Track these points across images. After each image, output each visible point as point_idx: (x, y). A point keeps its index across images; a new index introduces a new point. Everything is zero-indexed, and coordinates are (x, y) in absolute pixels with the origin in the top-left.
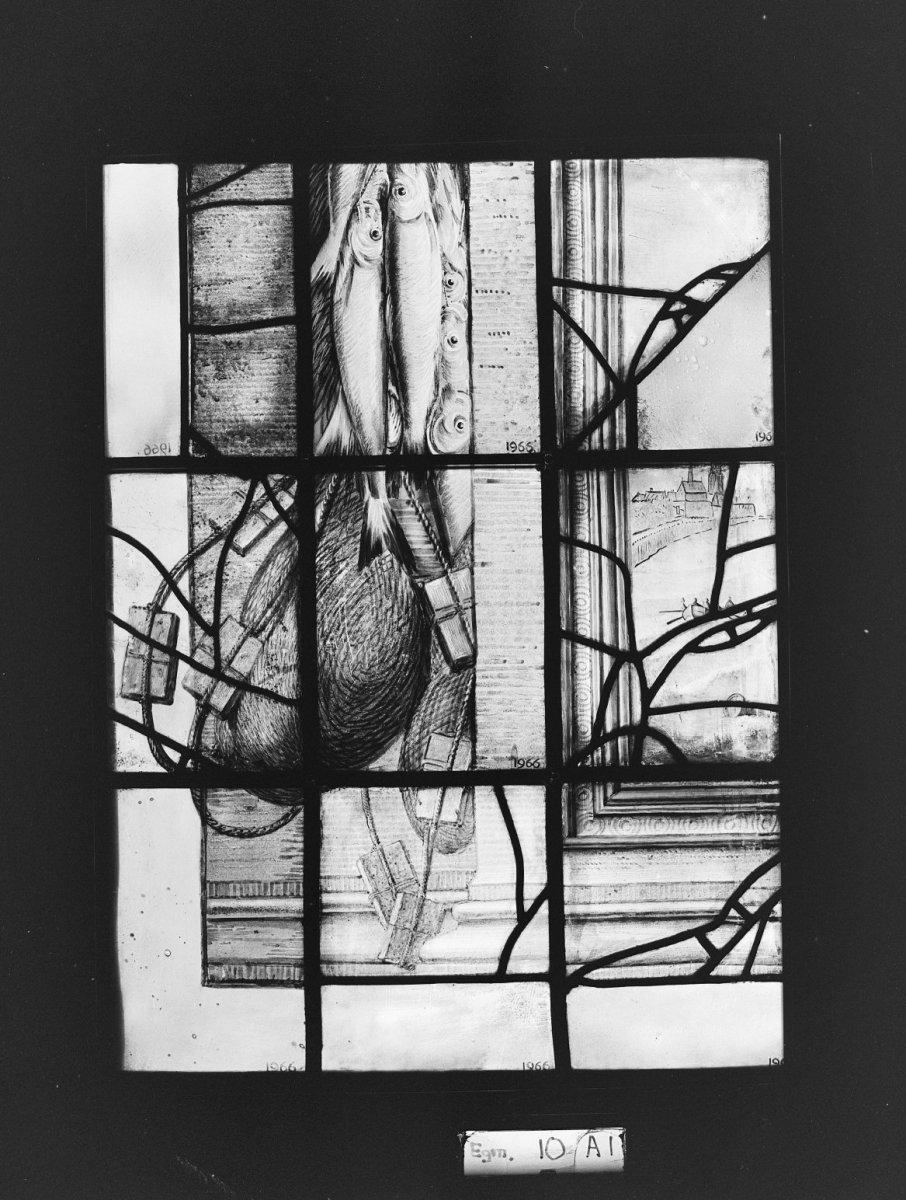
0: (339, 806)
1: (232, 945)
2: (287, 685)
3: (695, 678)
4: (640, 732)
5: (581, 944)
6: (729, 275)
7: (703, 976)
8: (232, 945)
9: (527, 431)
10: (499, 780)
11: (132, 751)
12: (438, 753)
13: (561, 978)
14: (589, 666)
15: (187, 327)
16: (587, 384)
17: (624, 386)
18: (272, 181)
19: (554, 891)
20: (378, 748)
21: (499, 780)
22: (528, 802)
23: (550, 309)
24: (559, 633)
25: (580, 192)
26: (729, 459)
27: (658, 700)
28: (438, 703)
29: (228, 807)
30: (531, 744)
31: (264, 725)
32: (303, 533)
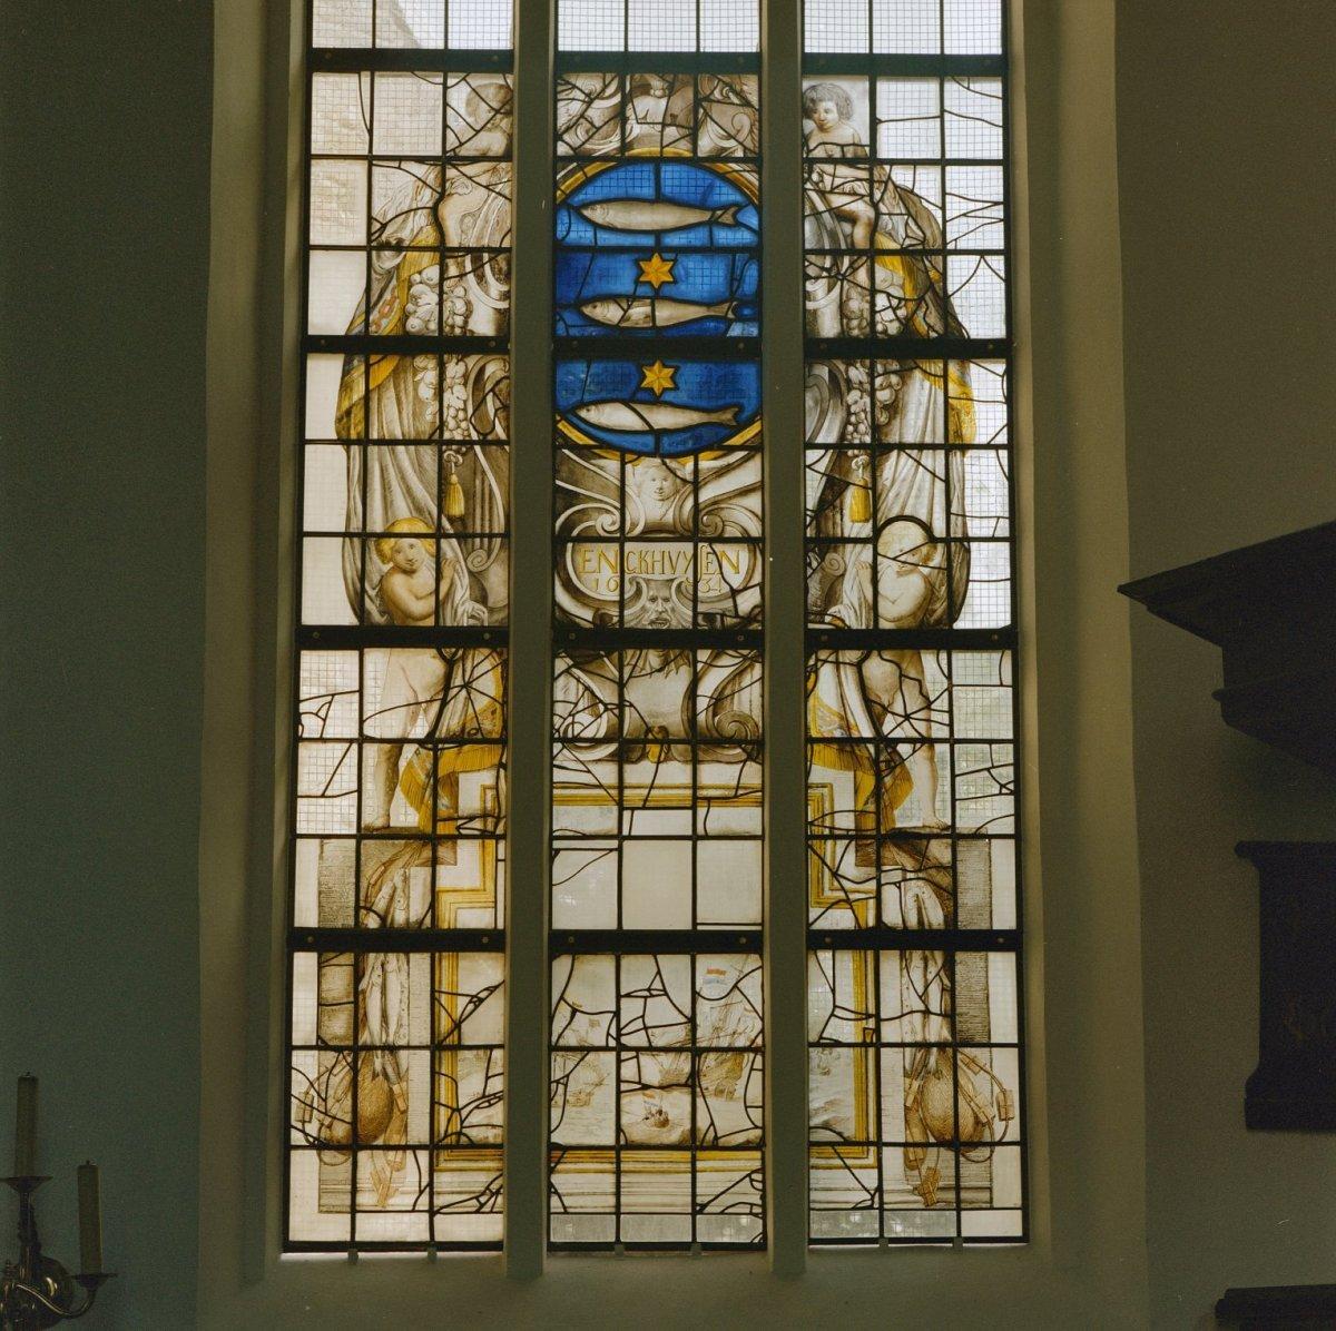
0: (363, 1156)
1: (328, 1200)
2: (348, 1118)
3: (477, 1117)
4: (459, 1134)
5: (439, 1201)
6: (491, 990)
7: (477, 1212)
8: (328, 1200)
9: (426, 1039)
10: (414, 1148)
11: (297, 1138)
12: (395, 1140)
13: (432, 1212)
14: (443, 1114)
15: (319, 1004)
16: (445, 1024)
17: (457, 1025)
18: (348, 958)
19: (431, 1184)
20: (376, 1138)
21: (414, 1148)
22: (423, 1156)
23: (433, 1000)
24: (434, 1103)
25: (445, 963)
26: (491, 1048)
27: (465, 1124)
28: (395, 1124)
29: (328, 1155)
30: (425, 1138)
31: (340, 1131)
32: (355, 1069)
